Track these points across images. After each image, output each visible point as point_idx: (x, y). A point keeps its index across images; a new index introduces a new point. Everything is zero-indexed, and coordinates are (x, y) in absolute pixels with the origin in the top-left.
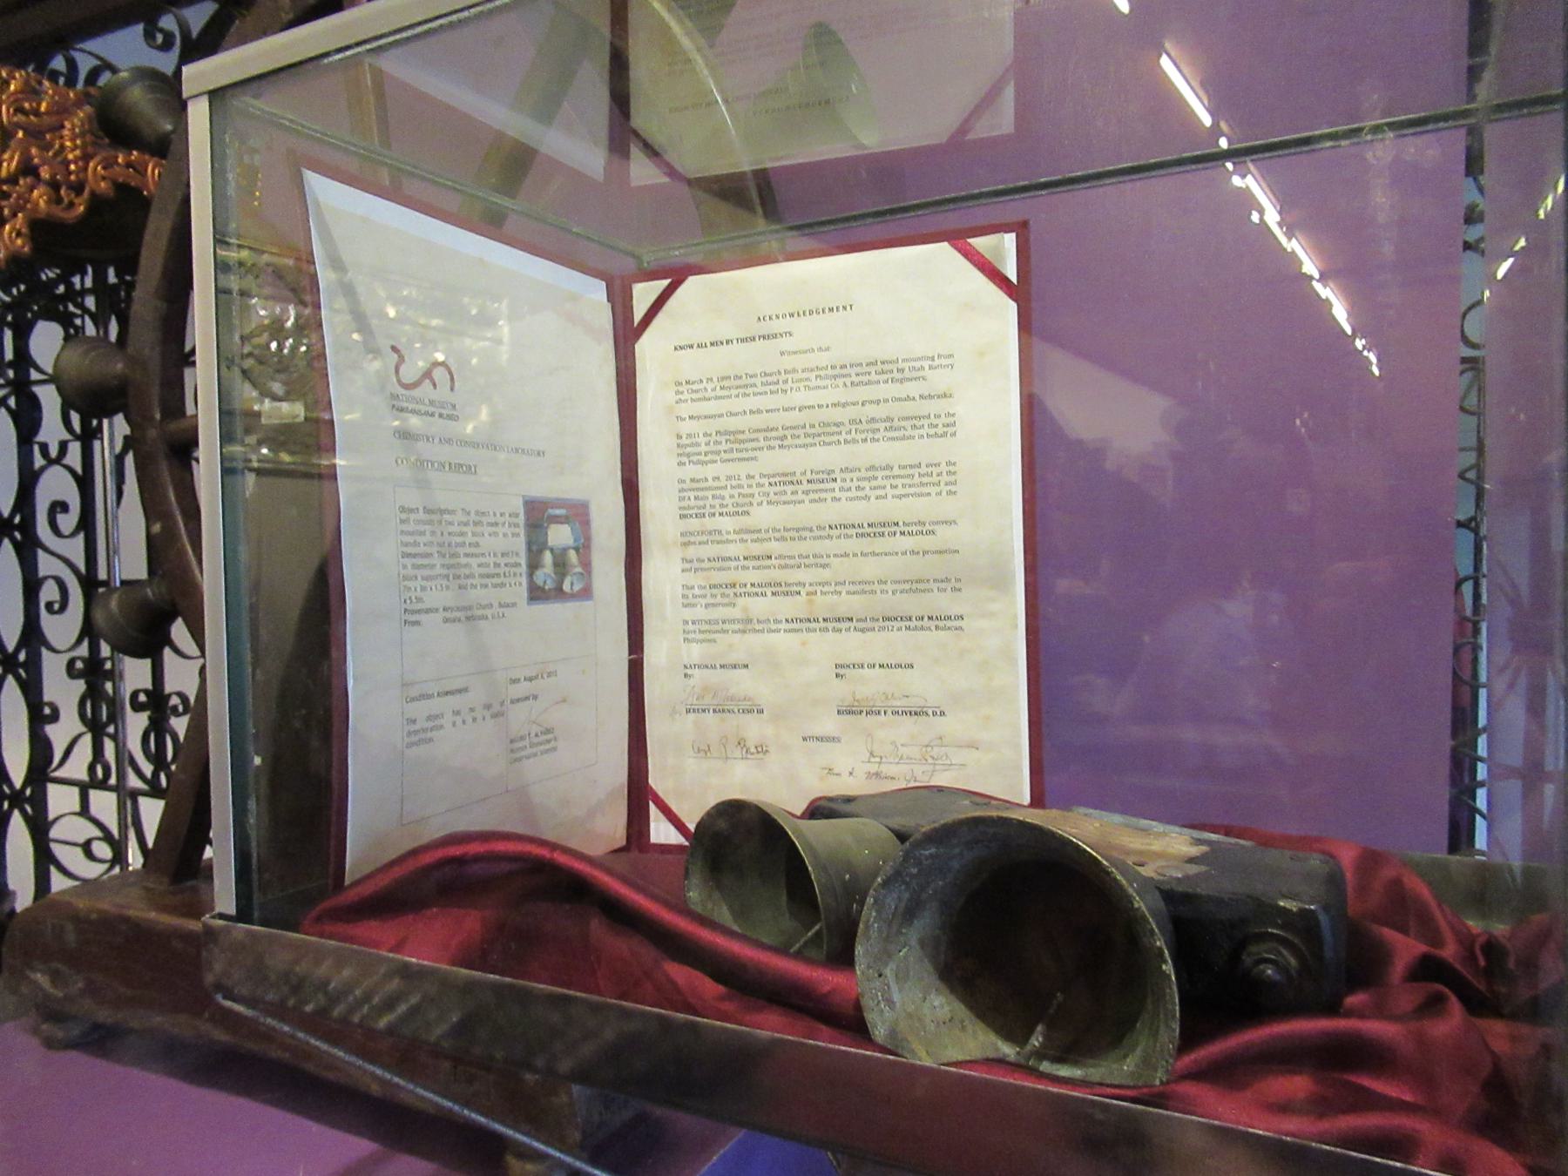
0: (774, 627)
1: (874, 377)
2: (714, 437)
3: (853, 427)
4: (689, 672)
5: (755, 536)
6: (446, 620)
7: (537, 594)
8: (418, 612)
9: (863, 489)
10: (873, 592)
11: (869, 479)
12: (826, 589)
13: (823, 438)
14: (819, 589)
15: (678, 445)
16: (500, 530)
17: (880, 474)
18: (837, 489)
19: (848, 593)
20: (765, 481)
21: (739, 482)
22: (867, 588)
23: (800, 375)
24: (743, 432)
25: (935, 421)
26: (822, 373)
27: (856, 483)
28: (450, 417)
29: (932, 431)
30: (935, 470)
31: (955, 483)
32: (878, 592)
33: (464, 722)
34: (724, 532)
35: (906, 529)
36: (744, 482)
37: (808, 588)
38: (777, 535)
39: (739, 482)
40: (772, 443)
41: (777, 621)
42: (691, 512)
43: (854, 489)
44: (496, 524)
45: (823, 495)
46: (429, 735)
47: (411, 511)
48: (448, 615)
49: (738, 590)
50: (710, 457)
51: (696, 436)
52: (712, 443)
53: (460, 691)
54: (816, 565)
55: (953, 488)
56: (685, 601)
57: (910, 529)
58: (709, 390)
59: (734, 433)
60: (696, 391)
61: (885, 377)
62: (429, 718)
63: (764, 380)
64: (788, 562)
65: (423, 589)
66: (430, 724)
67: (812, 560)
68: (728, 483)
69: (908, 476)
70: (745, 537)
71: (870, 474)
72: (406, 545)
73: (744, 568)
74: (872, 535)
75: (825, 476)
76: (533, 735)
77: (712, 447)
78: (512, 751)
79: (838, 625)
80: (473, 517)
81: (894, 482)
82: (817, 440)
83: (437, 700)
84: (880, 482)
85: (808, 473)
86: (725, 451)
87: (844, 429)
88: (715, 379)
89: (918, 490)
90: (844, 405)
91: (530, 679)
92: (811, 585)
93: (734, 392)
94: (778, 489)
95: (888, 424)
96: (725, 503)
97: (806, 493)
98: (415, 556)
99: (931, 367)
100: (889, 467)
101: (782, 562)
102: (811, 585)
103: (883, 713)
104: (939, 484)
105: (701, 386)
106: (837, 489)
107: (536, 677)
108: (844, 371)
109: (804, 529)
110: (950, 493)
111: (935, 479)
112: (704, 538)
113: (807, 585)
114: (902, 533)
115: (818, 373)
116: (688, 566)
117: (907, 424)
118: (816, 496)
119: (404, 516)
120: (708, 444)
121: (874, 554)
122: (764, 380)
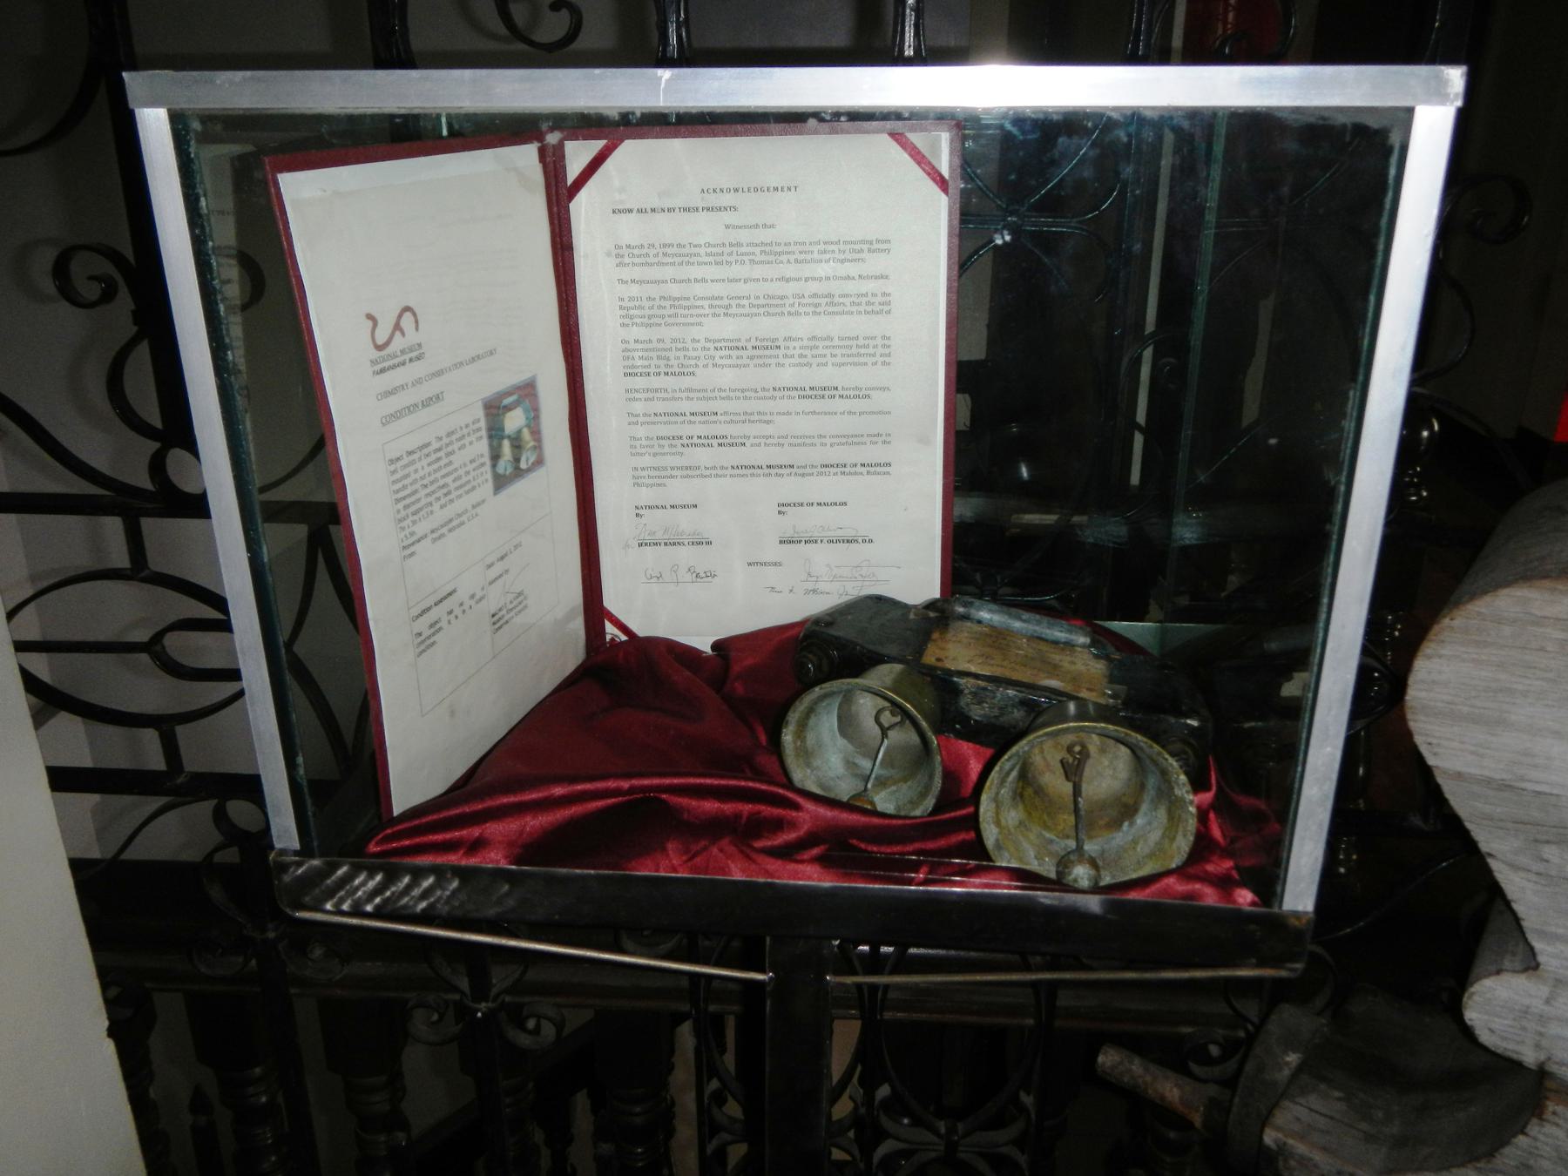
0: (720, 472)
1: (816, 256)
2: (657, 303)
3: (797, 301)
5: (701, 395)
6: (434, 540)
7: (500, 483)
8: (413, 544)
9: (806, 356)
11: (811, 348)
13: (767, 309)
14: (763, 441)
15: (621, 307)
16: (466, 441)
17: (821, 344)
18: (781, 356)
19: (790, 445)
20: (711, 345)
21: (684, 345)
23: (744, 249)
24: (688, 299)
25: (872, 300)
26: (768, 249)
27: (798, 352)
28: (418, 358)
29: (869, 308)
30: (872, 343)
31: (889, 355)
33: (456, 617)
34: (669, 390)
35: (845, 393)
36: (690, 345)
37: (752, 441)
38: (723, 394)
39: (684, 345)
40: (718, 311)
42: (635, 371)
43: (796, 356)
44: (463, 437)
45: (768, 361)
46: (432, 640)
47: (398, 459)
48: (434, 535)
49: (685, 441)
50: (653, 321)
51: (639, 299)
52: (655, 308)
53: (450, 594)
54: (760, 421)
55: (887, 360)
56: (634, 451)
57: (848, 393)
58: (651, 255)
59: (678, 299)
60: (639, 256)
61: (828, 256)
62: (431, 626)
63: (709, 250)
64: (734, 418)
65: (414, 522)
66: (433, 630)
67: (756, 417)
68: (673, 346)
69: (847, 347)
70: (691, 395)
71: (812, 343)
72: (398, 491)
73: (690, 422)
74: (813, 397)
75: (769, 344)
76: (508, 602)
77: (656, 311)
78: (494, 624)
79: (780, 471)
80: (446, 440)
81: (835, 351)
82: (762, 310)
83: (435, 609)
84: (820, 351)
85: (753, 340)
86: (669, 316)
87: (787, 302)
88: (657, 245)
89: (856, 360)
90: (788, 280)
91: (502, 558)
93: (678, 260)
94: (723, 353)
95: (829, 300)
96: (670, 363)
97: (752, 358)
98: (404, 498)
99: (869, 250)
100: (830, 338)
101: (728, 418)
103: (819, 541)
104: (874, 355)
105: (644, 251)
106: (781, 356)
107: (506, 555)
108: (786, 249)
109: (748, 390)
110: (884, 363)
111: (871, 351)
112: (650, 395)
113: (751, 438)
114: (841, 396)
115: (763, 249)
116: (634, 419)
117: (847, 301)
118: (760, 361)
119: (392, 468)
120: (652, 308)
121: (814, 413)
122: (709, 250)
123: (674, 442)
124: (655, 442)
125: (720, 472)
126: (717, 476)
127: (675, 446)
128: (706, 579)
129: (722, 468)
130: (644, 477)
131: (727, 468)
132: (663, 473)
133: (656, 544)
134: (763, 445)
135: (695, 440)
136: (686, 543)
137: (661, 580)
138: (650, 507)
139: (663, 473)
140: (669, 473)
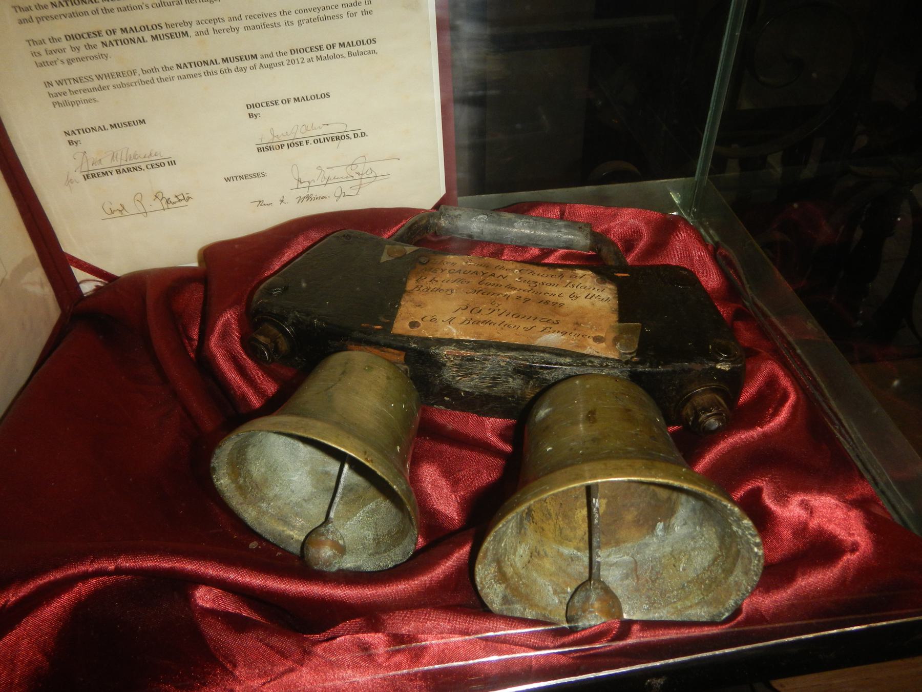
0: (164, 75)
4: (73, 138)
10: (275, 25)
12: (219, 26)
14: (210, 26)
22: (269, 20)
32: (283, 24)
41: (165, 68)
49: (106, 38)
56: (39, 60)
92: (199, 23)
102: (199, 23)
113: (194, 24)
116: (25, 15)
123: (92, 41)
124: (64, 44)
125: (164, 75)
126: (161, 80)
127: (95, 47)
128: (178, 204)
129: (165, 68)
130: (65, 94)
131: (171, 68)
132: (90, 85)
133: (105, 174)
134: (211, 32)
135: (119, 35)
136: (143, 167)
137: (124, 212)
139: (90, 85)
140: (96, 83)
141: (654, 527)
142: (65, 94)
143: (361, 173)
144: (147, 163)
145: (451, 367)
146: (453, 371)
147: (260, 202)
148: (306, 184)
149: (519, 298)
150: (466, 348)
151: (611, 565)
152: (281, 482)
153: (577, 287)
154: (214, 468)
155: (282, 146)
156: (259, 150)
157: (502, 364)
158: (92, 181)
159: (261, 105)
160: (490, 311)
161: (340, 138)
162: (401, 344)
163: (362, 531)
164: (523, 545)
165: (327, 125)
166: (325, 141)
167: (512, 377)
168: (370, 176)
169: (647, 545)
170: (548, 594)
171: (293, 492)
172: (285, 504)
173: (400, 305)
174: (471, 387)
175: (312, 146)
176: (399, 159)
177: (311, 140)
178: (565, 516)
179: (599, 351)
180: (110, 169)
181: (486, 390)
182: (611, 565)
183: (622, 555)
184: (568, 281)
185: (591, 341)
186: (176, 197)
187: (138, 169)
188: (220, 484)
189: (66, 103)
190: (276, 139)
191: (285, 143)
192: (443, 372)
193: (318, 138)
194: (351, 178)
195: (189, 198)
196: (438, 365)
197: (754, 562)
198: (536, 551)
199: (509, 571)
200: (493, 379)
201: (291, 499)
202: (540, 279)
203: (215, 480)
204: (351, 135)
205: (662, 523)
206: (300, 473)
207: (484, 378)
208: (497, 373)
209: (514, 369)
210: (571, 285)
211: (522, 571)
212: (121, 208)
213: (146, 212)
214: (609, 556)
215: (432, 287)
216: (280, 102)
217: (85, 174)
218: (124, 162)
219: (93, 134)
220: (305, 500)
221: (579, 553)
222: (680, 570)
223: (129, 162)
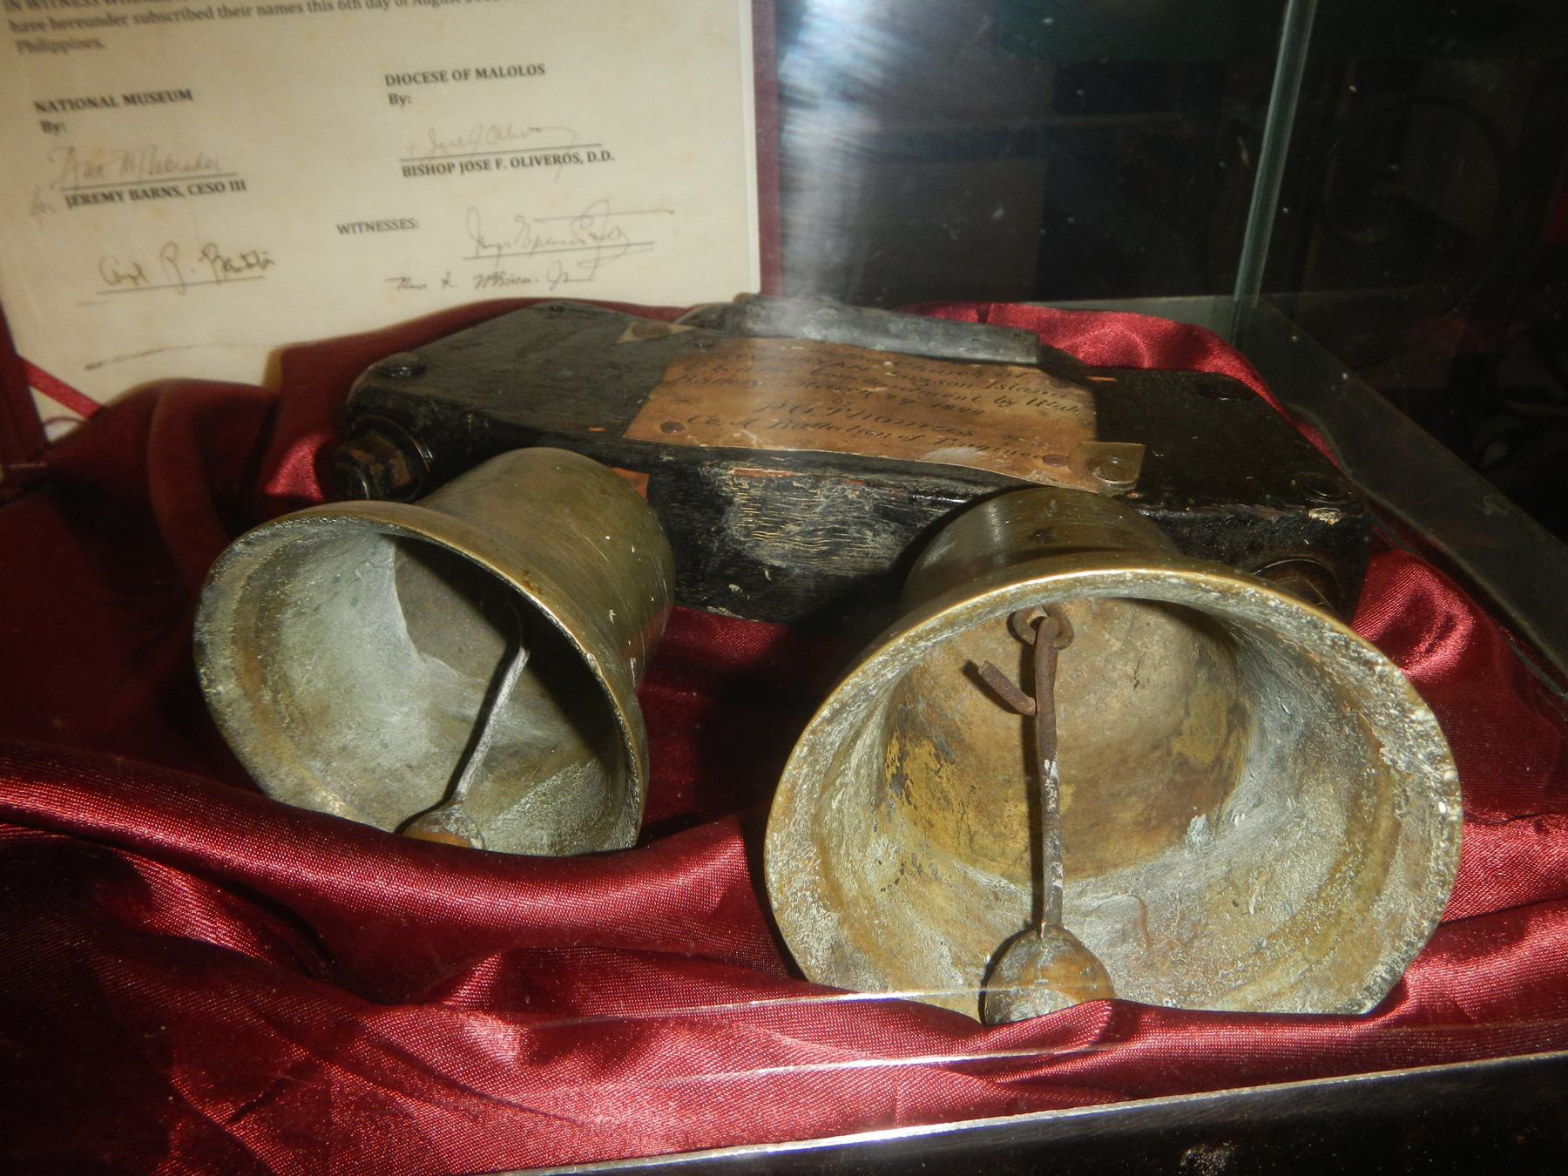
4: (52, 117)
128: (247, 273)
130: (41, 26)
133: (108, 197)
136: (183, 188)
137: (142, 283)
138: (74, 105)
141: (1184, 828)
142: (41, 26)
143: (599, 235)
144: (190, 182)
145: (744, 505)
146: (748, 515)
147: (404, 280)
148: (494, 251)
149: (890, 397)
150: (776, 465)
151: (1086, 914)
152: (360, 720)
153: (1010, 388)
154: (201, 645)
155: (450, 168)
156: (407, 172)
157: (850, 497)
158: (85, 211)
159: (413, 79)
160: (831, 411)
161: (561, 160)
162: (644, 459)
163: (527, 832)
164: (884, 839)
165: (538, 130)
166: (532, 164)
167: (870, 527)
168: (617, 242)
169: (1168, 868)
170: (939, 963)
171: (386, 746)
172: (365, 769)
173: (646, 399)
174: (783, 557)
175: (507, 173)
176: (672, 212)
177: (506, 160)
178: (980, 809)
179: (1057, 478)
180: (118, 189)
181: (816, 564)
182: (1086, 914)
183: (1111, 892)
184: (992, 381)
185: (1040, 463)
186: (244, 257)
187: (172, 192)
188: (215, 694)
189: (42, 46)
190: (439, 152)
191: (456, 162)
192: (727, 521)
193: (519, 156)
194: (579, 245)
195: (268, 262)
196: (717, 504)
197: (1438, 847)
198: (913, 863)
199: (850, 887)
200: (832, 532)
201: (380, 760)
202: (935, 377)
203: (205, 682)
204: (583, 156)
205: (1204, 817)
206: (405, 709)
207: (812, 533)
208: (840, 517)
209: (877, 509)
210: (999, 385)
211: (881, 898)
212: (134, 272)
213: (183, 285)
214: (1081, 894)
215: (716, 377)
216: (449, 76)
217: (70, 193)
218: (146, 177)
219: (88, 113)
220: (410, 767)
221: (1012, 886)
222: (1249, 912)
223: (157, 177)
